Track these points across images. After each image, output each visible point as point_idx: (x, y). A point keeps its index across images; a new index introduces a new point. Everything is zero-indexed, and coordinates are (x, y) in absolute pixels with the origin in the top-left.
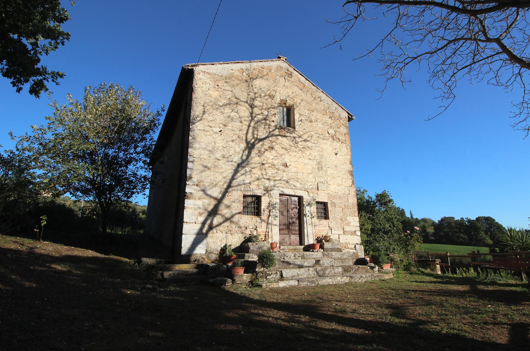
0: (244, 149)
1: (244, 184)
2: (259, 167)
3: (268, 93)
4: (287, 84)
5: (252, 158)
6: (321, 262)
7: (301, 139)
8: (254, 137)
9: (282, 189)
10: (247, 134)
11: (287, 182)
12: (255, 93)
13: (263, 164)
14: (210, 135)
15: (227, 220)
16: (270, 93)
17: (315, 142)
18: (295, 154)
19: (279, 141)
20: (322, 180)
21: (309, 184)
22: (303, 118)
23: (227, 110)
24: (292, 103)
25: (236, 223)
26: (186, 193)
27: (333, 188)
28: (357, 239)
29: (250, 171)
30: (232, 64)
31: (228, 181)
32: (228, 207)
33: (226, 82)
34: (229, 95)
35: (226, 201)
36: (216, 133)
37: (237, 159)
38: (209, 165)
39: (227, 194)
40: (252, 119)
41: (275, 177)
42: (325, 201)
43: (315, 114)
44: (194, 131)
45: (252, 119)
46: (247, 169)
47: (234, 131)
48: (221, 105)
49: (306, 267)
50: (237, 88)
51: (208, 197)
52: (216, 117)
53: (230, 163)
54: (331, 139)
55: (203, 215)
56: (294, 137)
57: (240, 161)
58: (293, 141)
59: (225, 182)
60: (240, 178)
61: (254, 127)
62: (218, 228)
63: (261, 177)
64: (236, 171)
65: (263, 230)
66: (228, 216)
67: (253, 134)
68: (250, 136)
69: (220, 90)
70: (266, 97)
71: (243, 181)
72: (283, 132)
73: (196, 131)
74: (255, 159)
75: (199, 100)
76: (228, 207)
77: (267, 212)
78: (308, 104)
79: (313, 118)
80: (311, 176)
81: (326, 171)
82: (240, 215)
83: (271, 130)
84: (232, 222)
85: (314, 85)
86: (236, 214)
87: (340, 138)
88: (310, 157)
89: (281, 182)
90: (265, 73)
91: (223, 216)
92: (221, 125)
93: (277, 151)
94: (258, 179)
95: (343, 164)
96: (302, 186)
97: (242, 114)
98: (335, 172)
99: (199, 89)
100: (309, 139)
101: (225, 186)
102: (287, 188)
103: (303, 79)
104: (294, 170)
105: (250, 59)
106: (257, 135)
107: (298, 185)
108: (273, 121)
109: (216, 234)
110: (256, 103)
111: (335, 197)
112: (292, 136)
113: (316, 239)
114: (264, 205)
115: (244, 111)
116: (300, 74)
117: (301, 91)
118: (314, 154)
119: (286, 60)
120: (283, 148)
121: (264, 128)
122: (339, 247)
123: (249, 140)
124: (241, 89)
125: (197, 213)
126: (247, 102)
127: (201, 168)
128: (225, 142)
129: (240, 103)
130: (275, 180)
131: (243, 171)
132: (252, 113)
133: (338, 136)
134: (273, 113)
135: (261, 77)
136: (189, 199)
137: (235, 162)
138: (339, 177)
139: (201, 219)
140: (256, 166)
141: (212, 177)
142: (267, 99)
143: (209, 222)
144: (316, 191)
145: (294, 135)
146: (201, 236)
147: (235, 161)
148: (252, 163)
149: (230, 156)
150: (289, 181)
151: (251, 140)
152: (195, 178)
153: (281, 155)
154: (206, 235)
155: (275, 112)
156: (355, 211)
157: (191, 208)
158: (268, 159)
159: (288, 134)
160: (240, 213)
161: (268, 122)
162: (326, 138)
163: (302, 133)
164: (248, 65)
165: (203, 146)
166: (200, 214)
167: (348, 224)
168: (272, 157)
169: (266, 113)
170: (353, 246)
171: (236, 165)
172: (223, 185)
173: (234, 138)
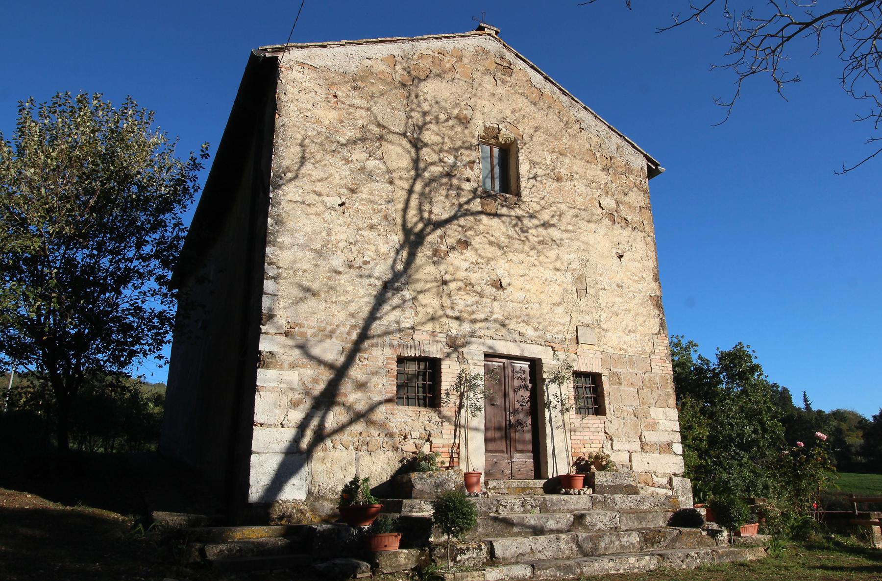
0: (398, 246)
1: (400, 331)
2: (435, 290)
3: (456, 111)
4: (501, 90)
5: (420, 267)
6: (588, 519)
7: (535, 222)
8: (422, 219)
9: (490, 342)
10: (405, 210)
11: (503, 325)
12: (425, 114)
13: (445, 283)
14: (317, 214)
15: (358, 417)
16: (460, 112)
17: (570, 227)
18: (522, 256)
19: (481, 227)
20: (587, 319)
22: (540, 172)
23: (358, 155)
24: (512, 136)
25: (381, 426)
26: (260, 353)
27: (614, 339)
28: (674, 463)
30: (369, 46)
31: (361, 323)
32: (361, 386)
33: (355, 88)
34: (362, 118)
35: (356, 372)
36: (331, 208)
37: (382, 270)
38: (315, 286)
39: (358, 355)
40: (418, 176)
41: (473, 312)
42: (596, 369)
43: (567, 161)
44: (279, 204)
45: (418, 176)
46: (407, 294)
47: (375, 203)
48: (343, 141)
49: (551, 531)
50: (382, 101)
51: (314, 364)
52: (331, 170)
53: (367, 281)
54: (606, 221)
55: (302, 407)
56: (519, 218)
57: (390, 276)
58: (516, 225)
59: (354, 327)
60: (389, 317)
61: (422, 194)
62: (337, 437)
63: (440, 313)
64: (380, 300)
65: (446, 442)
66: (361, 407)
67: (420, 211)
68: (412, 213)
69: (340, 106)
70: (451, 123)
71: (398, 322)
72: (492, 206)
73: (284, 204)
74: (425, 269)
75: (290, 132)
76: (361, 386)
77: (454, 398)
78: (550, 139)
79: (564, 172)
80: (560, 310)
81: (597, 298)
82: (389, 406)
83: (463, 200)
84: (370, 423)
85: (564, 93)
86: (380, 403)
87: (629, 218)
88: (558, 264)
89: (488, 324)
90: (448, 66)
91: (349, 408)
92: (344, 191)
93: (476, 250)
94: (433, 319)
95: (638, 282)
96: (539, 333)
97: (393, 164)
98: (620, 299)
99: (292, 105)
100: (554, 221)
101: (354, 336)
102: (502, 338)
103: (537, 78)
104: (518, 295)
105: (412, 32)
106: (430, 212)
107: (530, 332)
108: (468, 180)
109: (331, 453)
110: (428, 136)
111: (618, 361)
112: (513, 213)
113: (575, 464)
114: (447, 381)
115: (398, 155)
116: (532, 67)
117: (533, 108)
118: (566, 257)
119: (497, 33)
120: (491, 243)
121: (447, 196)
122: (630, 481)
123: (409, 225)
124: (390, 103)
125: (285, 400)
126: (404, 135)
127: (296, 293)
128: (351, 230)
129: (390, 137)
130: (474, 321)
131: (396, 301)
132: (416, 161)
133: (623, 214)
134: (466, 159)
135: (439, 75)
136: (267, 368)
137: (378, 278)
138: (629, 311)
139: (297, 416)
141: (322, 315)
142: (452, 128)
143: (315, 423)
144: (573, 347)
145: (519, 212)
146: (295, 458)
147: (376, 274)
148: (418, 280)
149: (366, 263)
150: (507, 322)
151: (416, 224)
152: (282, 317)
153: (489, 260)
154: (308, 455)
155: (472, 158)
156: (668, 395)
157: (272, 390)
158: (457, 269)
159: (504, 211)
160: (389, 401)
161: (455, 181)
162: (594, 218)
163: (538, 207)
164: (407, 46)
165: (302, 240)
166: (295, 404)
167: (653, 426)
168: (466, 265)
169: (450, 159)
170: (665, 481)
171: (379, 284)
172: (348, 333)
173: (375, 221)
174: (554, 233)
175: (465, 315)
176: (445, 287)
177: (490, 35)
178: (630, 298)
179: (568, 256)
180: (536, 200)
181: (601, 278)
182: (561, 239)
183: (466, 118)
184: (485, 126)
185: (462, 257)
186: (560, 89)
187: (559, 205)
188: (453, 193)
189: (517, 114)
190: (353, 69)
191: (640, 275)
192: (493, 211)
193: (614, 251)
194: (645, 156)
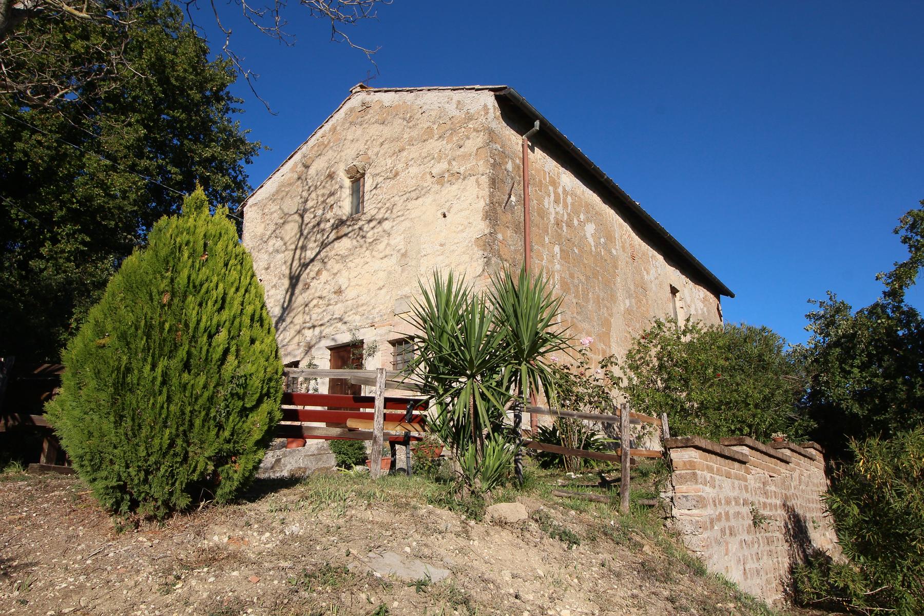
7: (372, 224)
10: (291, 265)
11: (340, 319)
17: (399, 214)
19: (333, 252)
21: (377, 310)
29: (292, 322)
30: (285, 167)
40: (302, 234)
43: (405, 154)
46: (288, 320)
67: (300, 259)
74: (300, 299)
79: (400, 166)
80: (383, 291)
85: (411, 91)
87: (462, 170)
88: (387, 252)
95: (462, 231)
98: (441, 258)
100: (387, 215)
103: (388, 98)
108: (329, 221)
110: (310, 204)
112: (356, 227)
115: (291, 230)
116: (386, 91)
117: (382, 127)
118: (392, 242)
119: (362, 87)
130: (321, 325)
133: (456, 169)
153: (335, 274)
159: (350, 229)
161: (322, 226)
174: (387, 225)
175: (316, 324)
176: (307, 309)
188: (319, 236)
190: (274, 190)
193: (439, 212)
194: (491, 90)
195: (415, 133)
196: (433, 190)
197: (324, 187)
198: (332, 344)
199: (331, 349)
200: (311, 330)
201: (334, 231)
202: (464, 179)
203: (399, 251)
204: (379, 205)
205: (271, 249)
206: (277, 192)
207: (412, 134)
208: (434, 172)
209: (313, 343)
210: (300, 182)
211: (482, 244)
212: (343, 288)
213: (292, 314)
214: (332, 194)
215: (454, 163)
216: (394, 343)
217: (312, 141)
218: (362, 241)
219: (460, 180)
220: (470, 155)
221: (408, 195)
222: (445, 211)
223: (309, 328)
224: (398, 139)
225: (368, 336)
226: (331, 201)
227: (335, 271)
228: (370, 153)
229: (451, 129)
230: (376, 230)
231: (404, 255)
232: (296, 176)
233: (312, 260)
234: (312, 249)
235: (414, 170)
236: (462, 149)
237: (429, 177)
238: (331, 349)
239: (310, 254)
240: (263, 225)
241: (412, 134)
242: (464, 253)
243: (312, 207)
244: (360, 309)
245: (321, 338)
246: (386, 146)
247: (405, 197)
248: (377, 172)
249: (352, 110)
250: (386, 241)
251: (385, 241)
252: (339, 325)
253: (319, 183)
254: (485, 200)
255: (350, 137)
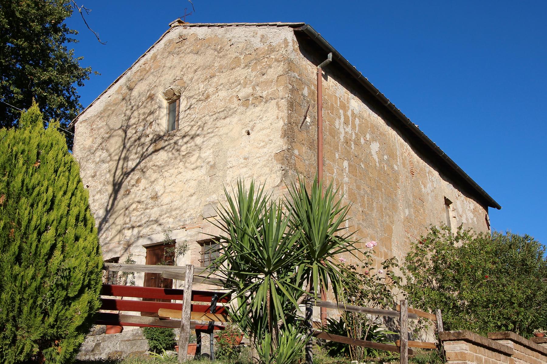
7: (185, 140)
17: (210, 131)
21: (188, 214)
29: (114, 223)
40: (124, 147)
43: (215, 79)
67: (122, 168)
74: (121, 203)
79: (211, 90)
85: (222, 26)
87: (264, 94)
88: (198, 164)
90: (147, 69)
95: (264, 147)
98: (245, 170)
100: (198, 132)
103: (202, 32)
108: (148, 136)
110: (132, 121)
112: (172, 141)
115: (115, 143)
116: (200, 26)
117: (196, 56)
118: (203, 155)
119: (179, 22)
130: (139, 226)
133: (259, 94)
135: (141, 80)
140: (121, 212)
159: (167, 143)
161: (142, 140)
163: (190, 128)
164: (129, 74)
174: (198, 140)
175: (134, 225)
176: (127, 212)
177: (174, 27)
178: (256, 164)
179: (206, 154)
180: (188, 123)
181: (230, 159)
182: (203, 142)
183: (154, 95)
184: (164, 93)
185: (138, 189)
186: (219, 26)
187: (204, 119)
188: (139, 149)
189: (184, 70)
190: (102, 108)
191: (267, 140)
192: (160, 147)
195: (224, 62)
196: (239, 111)
197: (145, 107)
198: (148, 242)
199: (147, 247)
200: (130, 231)
201: (153, 145)
202: (266, 102)
203: (209, 162)
204: (192, 123)
205: (97, 160)
206: (105, 110)
207: (222, 62)
208: (240, 95)
209: (131, 242)
210: (124, 102)
211: (280, 158)
212: (159, 194)
213: (114, 216)
214: (151, 113)
215: (258, 88)
216: (202, 243)
217: (136, 68)
218: (176, 154)
219: (263, 103)
220: (272, 82)
221: (217, 115)
222: (249, 129)
223: (129, 229)
224: (210, 67)
225: (179, 236)
226: (150, 118)
227: (153, 179)
228: (185, 78)
229: (255, 58)
230: (189, 145)
231: (213, 167)
232: (121, 97)
233: (133, 170)
234: (133, 160)
235: (223, 94)
236: (265, 77)
237: (235, 99)
238: (147, 247)
239: (131, 164)
240: (91, 139)
241: (222, 62)
242: (265, 166)
243: (134, 124)
244: (174, 213)
245: (139, 237)
246: (199, 73)
247: (214, 117)
248: (191, 95)
249: (170, 41)
250: (198, 155)
251: (196, 154)
252: (155, 226)
253: (140, 104)
254: (284, 121)
255: (168, 65)
